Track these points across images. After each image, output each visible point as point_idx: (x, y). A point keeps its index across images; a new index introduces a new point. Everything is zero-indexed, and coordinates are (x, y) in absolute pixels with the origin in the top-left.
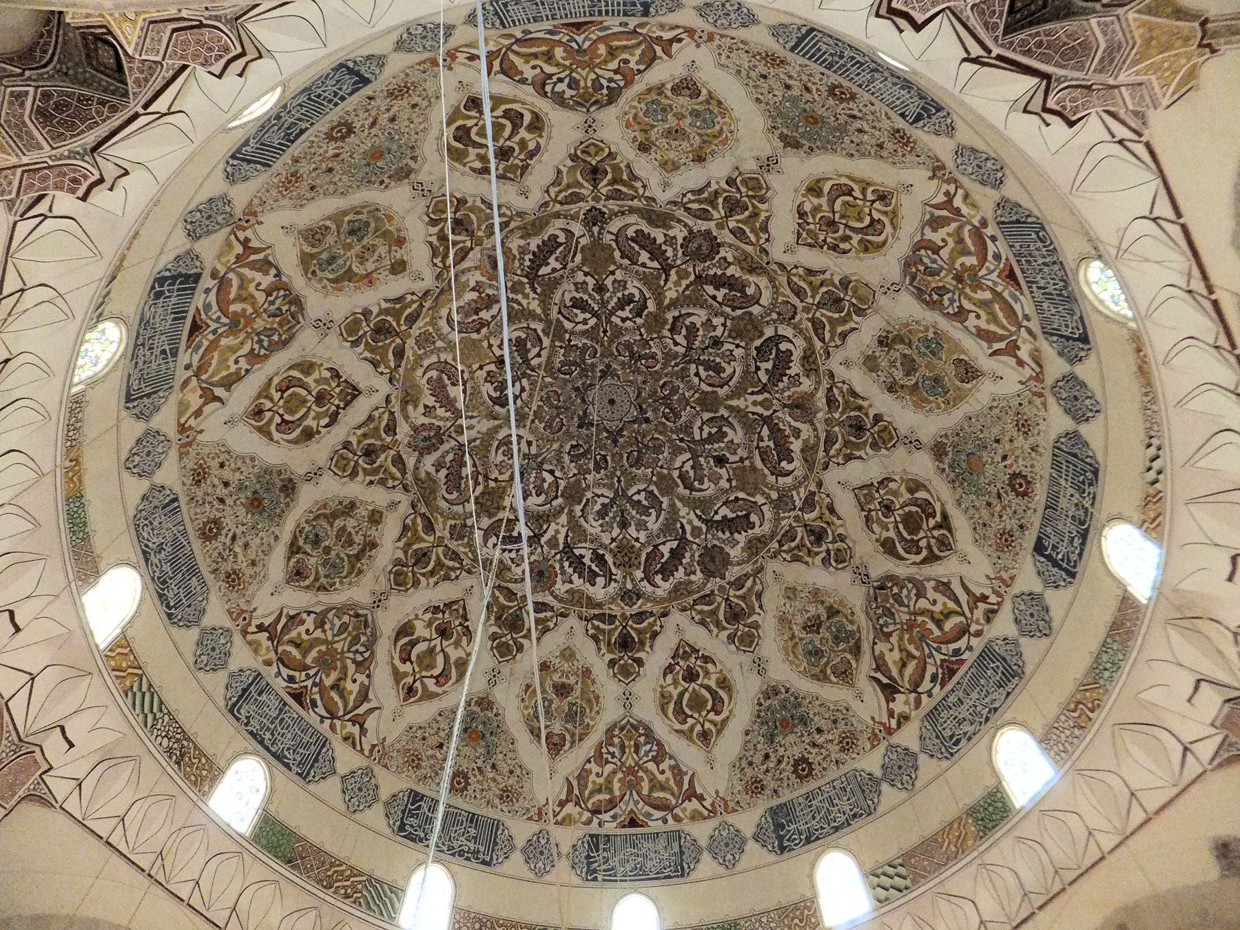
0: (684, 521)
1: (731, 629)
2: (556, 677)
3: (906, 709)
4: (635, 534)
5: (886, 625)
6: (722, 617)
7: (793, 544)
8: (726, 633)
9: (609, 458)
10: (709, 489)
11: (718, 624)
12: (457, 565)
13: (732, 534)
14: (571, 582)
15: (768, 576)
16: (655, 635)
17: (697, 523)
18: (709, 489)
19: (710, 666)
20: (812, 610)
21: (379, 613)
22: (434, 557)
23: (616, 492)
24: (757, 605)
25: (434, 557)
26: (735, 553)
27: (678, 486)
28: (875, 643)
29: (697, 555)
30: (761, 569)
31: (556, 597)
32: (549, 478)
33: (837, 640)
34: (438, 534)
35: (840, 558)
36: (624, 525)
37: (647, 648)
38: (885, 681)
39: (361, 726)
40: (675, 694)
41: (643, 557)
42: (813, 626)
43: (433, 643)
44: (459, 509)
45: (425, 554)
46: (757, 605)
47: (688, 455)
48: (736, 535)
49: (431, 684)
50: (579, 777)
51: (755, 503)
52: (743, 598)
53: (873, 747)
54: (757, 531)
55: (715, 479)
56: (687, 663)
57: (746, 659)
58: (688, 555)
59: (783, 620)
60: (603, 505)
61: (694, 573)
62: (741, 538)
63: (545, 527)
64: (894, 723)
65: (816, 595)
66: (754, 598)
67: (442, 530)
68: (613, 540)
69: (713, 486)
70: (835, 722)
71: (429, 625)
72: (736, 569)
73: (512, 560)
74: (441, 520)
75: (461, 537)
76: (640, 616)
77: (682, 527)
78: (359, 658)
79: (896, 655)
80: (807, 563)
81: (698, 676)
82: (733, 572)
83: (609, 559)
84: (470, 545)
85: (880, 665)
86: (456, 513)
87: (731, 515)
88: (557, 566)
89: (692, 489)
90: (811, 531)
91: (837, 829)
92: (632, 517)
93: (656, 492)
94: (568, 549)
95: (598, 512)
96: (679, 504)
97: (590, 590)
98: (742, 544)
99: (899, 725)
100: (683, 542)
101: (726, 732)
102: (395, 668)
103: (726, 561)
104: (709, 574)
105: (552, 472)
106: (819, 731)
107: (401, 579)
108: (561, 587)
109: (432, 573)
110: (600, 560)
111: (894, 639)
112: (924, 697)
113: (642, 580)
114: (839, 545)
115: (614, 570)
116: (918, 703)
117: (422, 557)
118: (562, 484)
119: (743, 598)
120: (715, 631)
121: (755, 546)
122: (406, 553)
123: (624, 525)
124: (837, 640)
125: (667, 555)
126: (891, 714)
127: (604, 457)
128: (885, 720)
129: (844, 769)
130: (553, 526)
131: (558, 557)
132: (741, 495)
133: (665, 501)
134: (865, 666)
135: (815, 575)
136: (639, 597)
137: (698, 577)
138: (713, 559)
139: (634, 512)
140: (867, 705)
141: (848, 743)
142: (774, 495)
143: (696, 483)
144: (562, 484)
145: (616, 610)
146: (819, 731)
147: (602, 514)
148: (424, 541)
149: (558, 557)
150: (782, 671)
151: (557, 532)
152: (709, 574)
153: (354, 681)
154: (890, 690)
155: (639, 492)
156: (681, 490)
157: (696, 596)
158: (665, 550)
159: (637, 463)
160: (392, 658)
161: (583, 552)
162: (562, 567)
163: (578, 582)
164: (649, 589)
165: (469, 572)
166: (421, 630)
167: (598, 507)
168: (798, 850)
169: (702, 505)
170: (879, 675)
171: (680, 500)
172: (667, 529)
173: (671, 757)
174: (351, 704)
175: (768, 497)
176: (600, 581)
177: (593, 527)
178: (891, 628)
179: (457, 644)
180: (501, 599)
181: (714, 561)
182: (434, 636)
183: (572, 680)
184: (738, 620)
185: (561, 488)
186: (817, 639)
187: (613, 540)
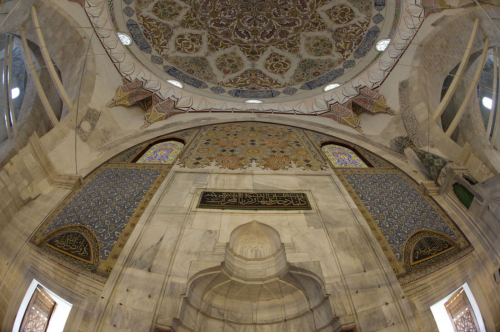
0: (274, 25)
1: (289, 49)
2: (229, 58)
3: (349, 53)
4: (259, 27)
5: (339, 39)
6: (286, 47)
7: (309, 28)
8: (288, 50)
9: (252, 9)
10: (282, 16)
11: (285, 48)
12: (201, 27)
13: (289, 27)
14: (237, 37)
15: (301, 36)
16: (263, 51)
17: (278, 25)
18: (282, 16)
19: (283, 58)
20: (316, 41)
21: (175, 30)
22: (194, 23)
23: (253, 17)
24: (298, 43)
25: (194, 23)
26: (291, 31)
27: (273, 16)
28: (336, 44)
29: (278, 32)
30: (299, 34)
31: (231, 40)
32: (233, 12)
33: (324, 46)
34: (197, 18)
35: (324, 28)
36: (255, 25)
37: (261, 54)
38: (341, 50)
39: (162, 50)
40: (270, 64)
41: (261, 33)
42: (317, 44)
43: (189, 42)
44: (205, 14)
45: (192, 22)
46: (298, 43)
47: (276, 8)
48: (291, 27)
49: (186, 50)
50: (234, 79)
51: (297, 19)
52: (294, 42)
53: (339, 64)
54: (297, 26)
55: (284, 14)
56: (274, 57)
57: (295, 55)
58: (275, 33)
59: (307, 45)
60: (249, 20)
61: (277, 37)
62: (293, 28)
63: (230, 23)
64: (345, 57)
65: (317, 38)
66: (297, 41)
67: (199, 17)
68: (251, 28)
69: (283, 16)
70: (326, 63)
71: (189, 37)
72: (291, 35)
73: (218, 29)
74: (198, 15)
75: (204, 20)
76: (259, 47)
77: (274, 26)
78: (166, 36)
79: (343, 44)
80: (313, 31)
81: (279, 60)
82: (290, 36)
83: (250, 33)
84: (206, 23)
85: (338, 47)
86: (204, 14)
87: (289, 23)
88: (233, 33)
89: (277, 17)
90: (313, 23)
91: (330, 81)
92: (258, 23)
93: (266, 17)
94: (237, 29)
95: (247, 21)
96: (273, 20)
97: (243, 40)
98: (293, 29)
99: (347, 57)
100: (274, 29)
101: (289, 71)
102: (176, 43)
103: (288, 34)
104: (282, 37)
105: (234, 10)
106: (321, 66)
107: (183, 24)
108: (233, 38)
109: (193, 26)
110: (247, 33)
111: (342, 41)
112: (354, 49)
113: (260, 38)
114: (323, 25)
115: (251, 36)
116: (352, 51)
117: (191, 22)
118: (237, 13)
119: (294, 42)
120: (284, 50)
121: (296, 30)
122: (187, 19)
123: (255, 25)
124: (324, 46)
125: (268, 33)
126: (344, 56)
127: (251, 9)
128: (342, 57)
129: (330, 71)
130: (233, 23)
131: (233, 31)
132: (292, 17)
133: (269, 20)
134: (334, 47)
135: (317, 33)
136: (259, 42)
137: (279, 38)
138: (283, 34)
139: (259, 22)
140: (336, 56)
141: (331, 65)
142: (302, 17)
143: (278, 15)
144: (237, 13)
145: (251, 45)
146: (321, 66)
147: (248, 22)
148: (192, 18)
149: (233, 31)
150: (306, 56)
151: (234, 25)
152: (282, 37)
153: (163, 40)
154: (343, 52)
155: (260, 17)
156: (274, 17)
157: (278, 42)
158: (268, 32)
159: (261, 10)
160: (176, 41)
161: (241, 30)
162: (234, 33)
163: (239, 37)
164: (262, 40)
165: (204, 29)
166: (186, 37)
167: (247, 20)
168: (316, 88)
169: (280, 21)
170: (339, 50)
171: (273, 19)
172: (269, 26)
173: (268, 77)
174: (160, 44)
175: (300, 17)
176: (246, 38)
177: (246, 25)
178: (341, 39)
179: (197, 44)
180: (213, 38)
181: (283, 34)
182: (190, 40)
183: (234, 59)
184: (293, 47)
185: (236, 14)
186: (318, 48)
187: (251, 28)
